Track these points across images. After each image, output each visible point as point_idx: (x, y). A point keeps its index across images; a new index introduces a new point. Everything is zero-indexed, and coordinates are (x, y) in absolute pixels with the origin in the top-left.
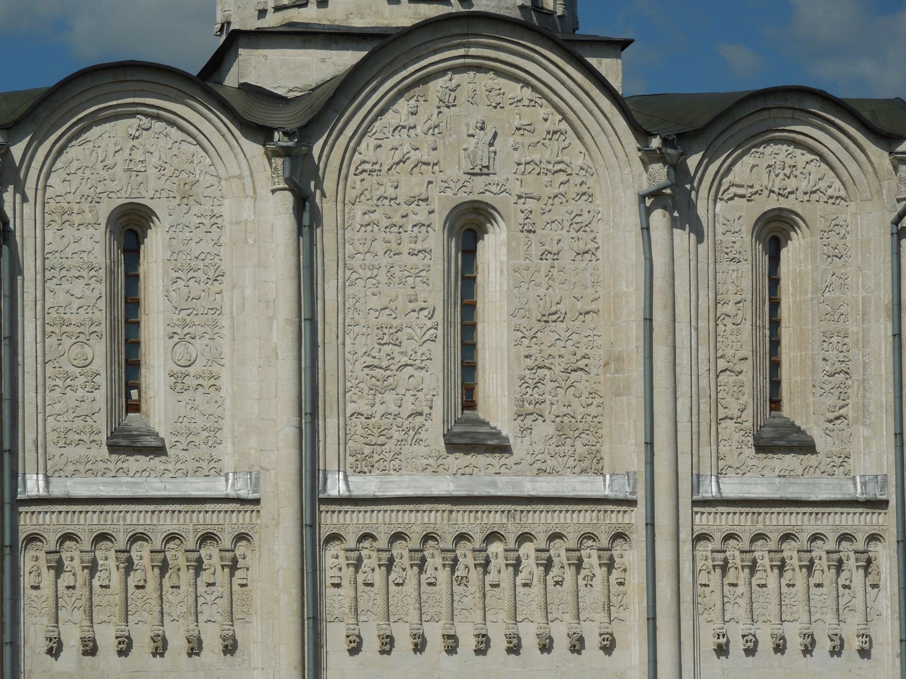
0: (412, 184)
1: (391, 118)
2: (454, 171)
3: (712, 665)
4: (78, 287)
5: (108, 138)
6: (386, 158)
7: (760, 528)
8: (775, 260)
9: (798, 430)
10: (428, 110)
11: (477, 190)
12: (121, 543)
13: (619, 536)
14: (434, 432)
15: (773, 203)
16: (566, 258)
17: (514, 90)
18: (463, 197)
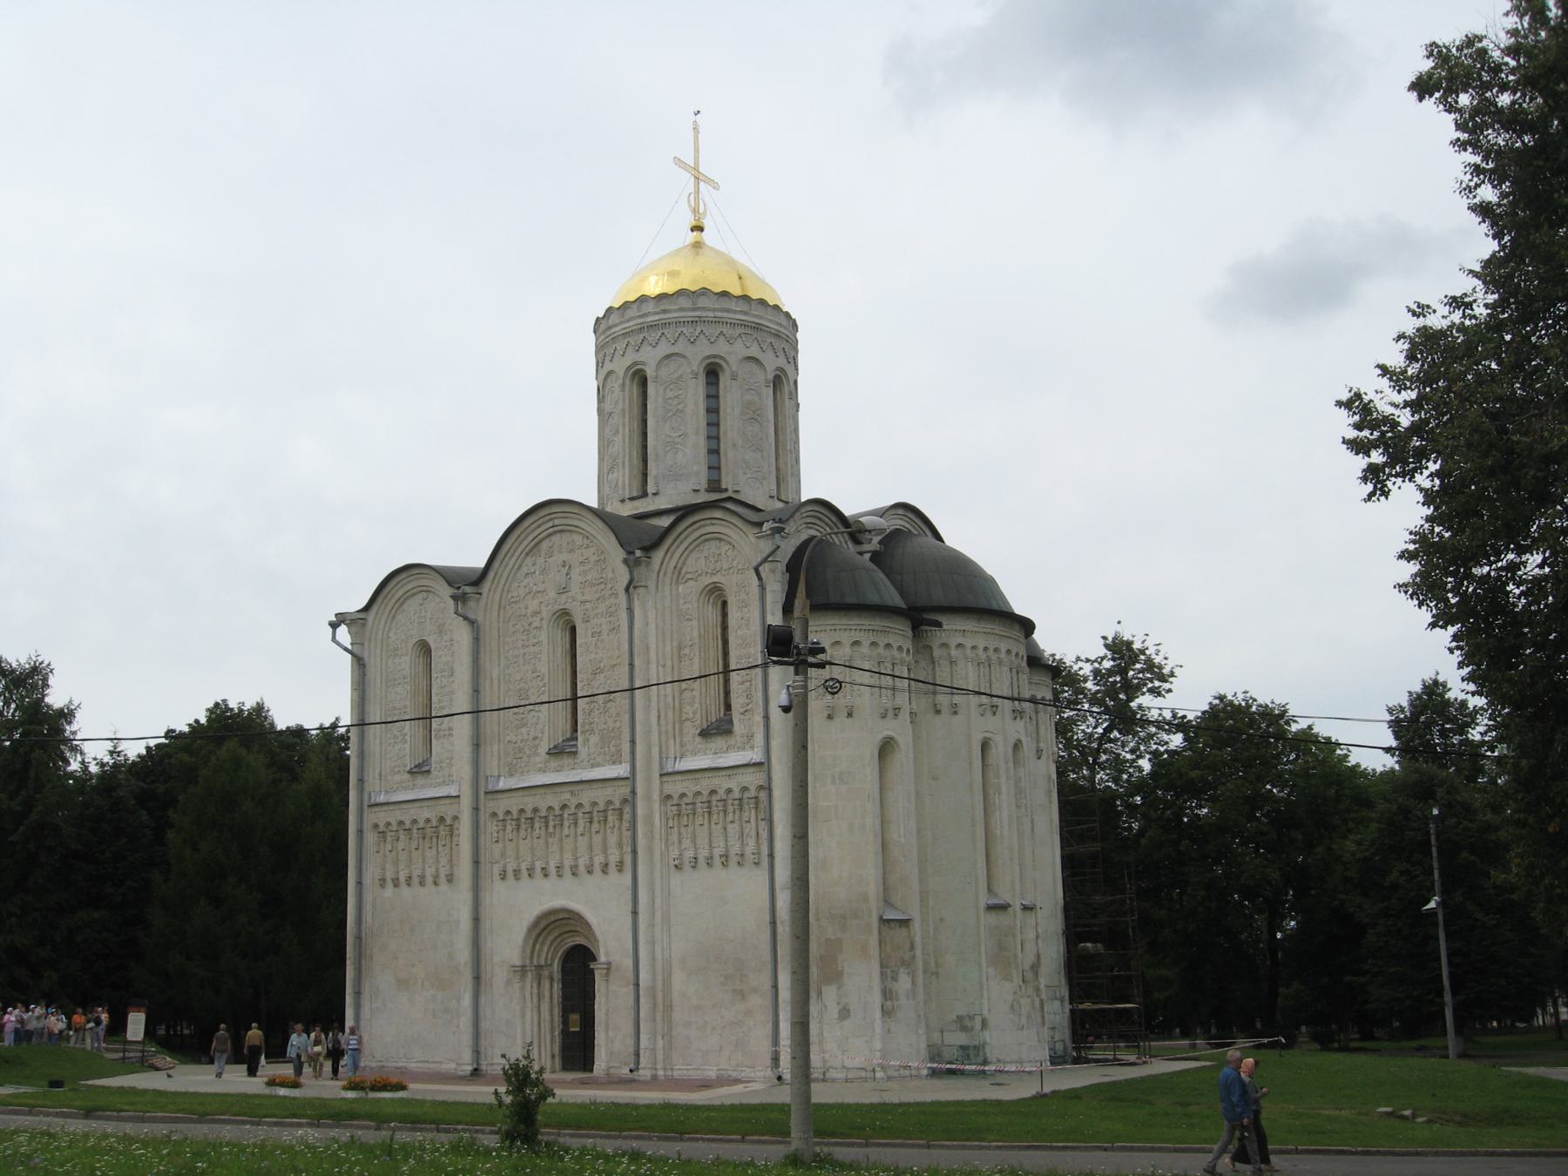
0: (533, 604)
1: (524, 570)
2: (552, 594)
3: (676, 879)
4: (399, 689)
5: (412, 606)
6: (522, 592)
7: (698, 788)
8: (724, 615)
9: (731, 722)
10: (540, 561)
11: (563, 602)
12: (408, 824)
13: (625, 801)
14: (544, 748)
15: (708, 580)
16: (605, 633)
17: (578, 539)
18: (557, 607)
